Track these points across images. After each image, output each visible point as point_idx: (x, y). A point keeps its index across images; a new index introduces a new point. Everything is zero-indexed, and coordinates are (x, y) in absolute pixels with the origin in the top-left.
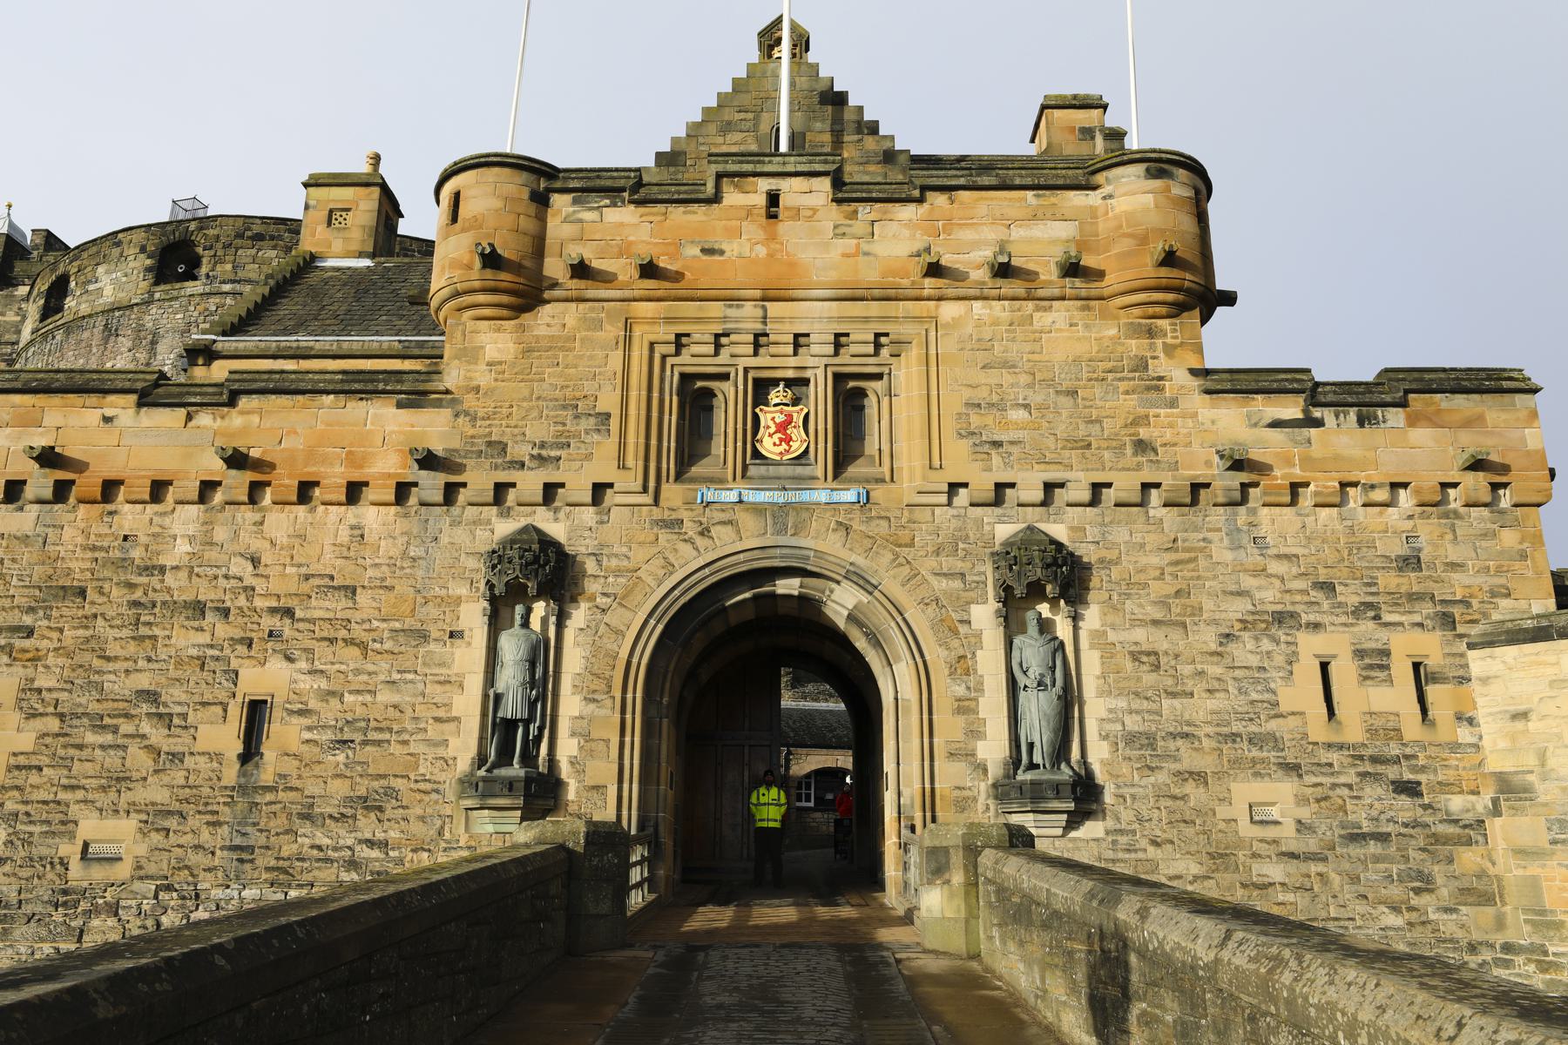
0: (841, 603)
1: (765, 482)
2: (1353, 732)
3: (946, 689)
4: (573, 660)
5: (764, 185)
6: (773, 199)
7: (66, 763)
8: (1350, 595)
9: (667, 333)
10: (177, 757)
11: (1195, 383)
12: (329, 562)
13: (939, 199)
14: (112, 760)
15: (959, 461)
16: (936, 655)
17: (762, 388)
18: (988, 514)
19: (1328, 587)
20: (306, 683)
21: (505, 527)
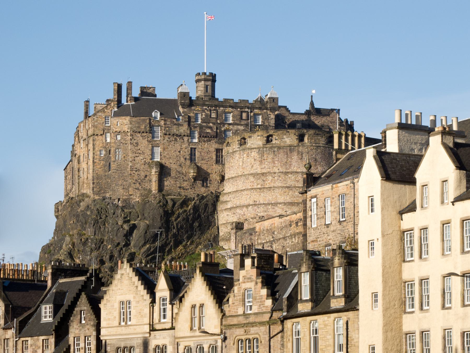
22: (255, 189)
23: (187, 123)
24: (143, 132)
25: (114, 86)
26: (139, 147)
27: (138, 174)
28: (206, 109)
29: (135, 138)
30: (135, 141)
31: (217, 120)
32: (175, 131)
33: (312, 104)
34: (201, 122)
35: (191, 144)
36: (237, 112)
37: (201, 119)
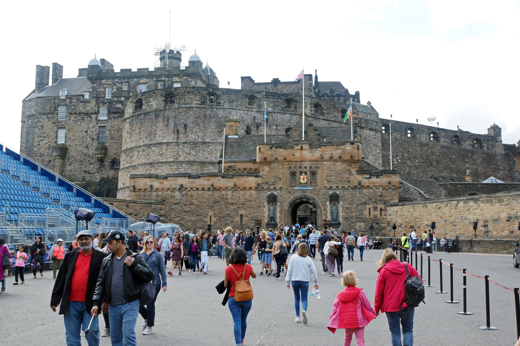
0: (311, 202)
1: (301, 186)
2: (372, 217)
3: (323, 212)
4: (278, 209)
5: (300, 145)
6: (302, 147)
7: (220, 222)
8: (373, 200)
9: (288, 166)
10: (233, 222)
11: (356, 173)
12: (248, 197)
13: (324, 147)
14: (225, 222)
15: (325, 183)
16: (322, 208)
17: (301, 173)
18: (329, 190)
19: (370, 199)
20: (247, 213)
21: (269, 193)
22: (124, 168)
23: (95, 99)
24: (48, 113)
25: (37, 69)
26: (44, 130)
27: (42, 160)
28: (117, 82)
29: (41, 120)
30: (41, 124)
31: (130, 93)
32: (81, 109)
33: (316, 78)
34: (112, 97)
35: (99, 122)
36: (152, 82)
37: (112, 94)
